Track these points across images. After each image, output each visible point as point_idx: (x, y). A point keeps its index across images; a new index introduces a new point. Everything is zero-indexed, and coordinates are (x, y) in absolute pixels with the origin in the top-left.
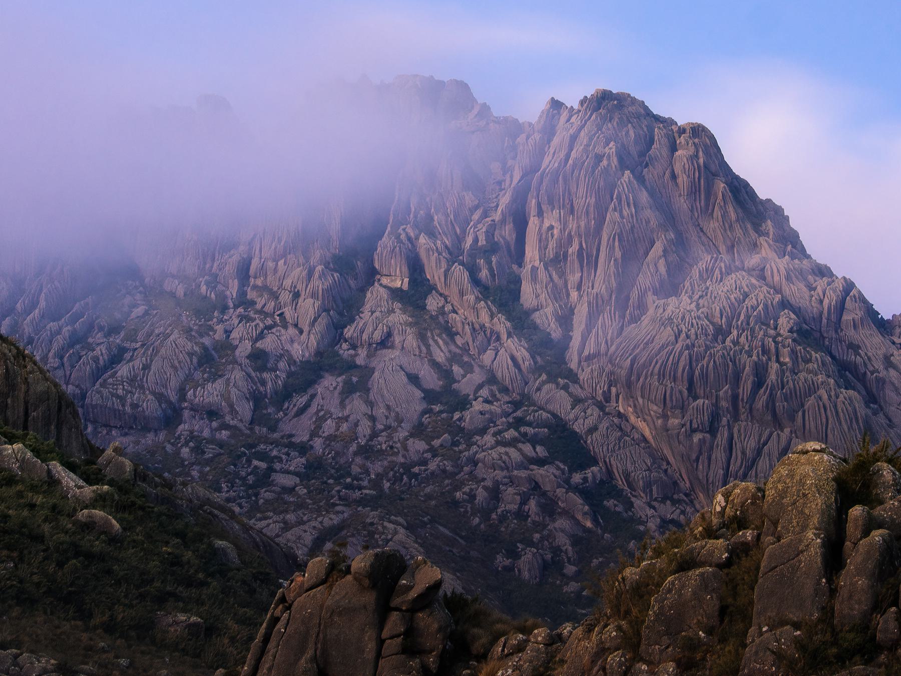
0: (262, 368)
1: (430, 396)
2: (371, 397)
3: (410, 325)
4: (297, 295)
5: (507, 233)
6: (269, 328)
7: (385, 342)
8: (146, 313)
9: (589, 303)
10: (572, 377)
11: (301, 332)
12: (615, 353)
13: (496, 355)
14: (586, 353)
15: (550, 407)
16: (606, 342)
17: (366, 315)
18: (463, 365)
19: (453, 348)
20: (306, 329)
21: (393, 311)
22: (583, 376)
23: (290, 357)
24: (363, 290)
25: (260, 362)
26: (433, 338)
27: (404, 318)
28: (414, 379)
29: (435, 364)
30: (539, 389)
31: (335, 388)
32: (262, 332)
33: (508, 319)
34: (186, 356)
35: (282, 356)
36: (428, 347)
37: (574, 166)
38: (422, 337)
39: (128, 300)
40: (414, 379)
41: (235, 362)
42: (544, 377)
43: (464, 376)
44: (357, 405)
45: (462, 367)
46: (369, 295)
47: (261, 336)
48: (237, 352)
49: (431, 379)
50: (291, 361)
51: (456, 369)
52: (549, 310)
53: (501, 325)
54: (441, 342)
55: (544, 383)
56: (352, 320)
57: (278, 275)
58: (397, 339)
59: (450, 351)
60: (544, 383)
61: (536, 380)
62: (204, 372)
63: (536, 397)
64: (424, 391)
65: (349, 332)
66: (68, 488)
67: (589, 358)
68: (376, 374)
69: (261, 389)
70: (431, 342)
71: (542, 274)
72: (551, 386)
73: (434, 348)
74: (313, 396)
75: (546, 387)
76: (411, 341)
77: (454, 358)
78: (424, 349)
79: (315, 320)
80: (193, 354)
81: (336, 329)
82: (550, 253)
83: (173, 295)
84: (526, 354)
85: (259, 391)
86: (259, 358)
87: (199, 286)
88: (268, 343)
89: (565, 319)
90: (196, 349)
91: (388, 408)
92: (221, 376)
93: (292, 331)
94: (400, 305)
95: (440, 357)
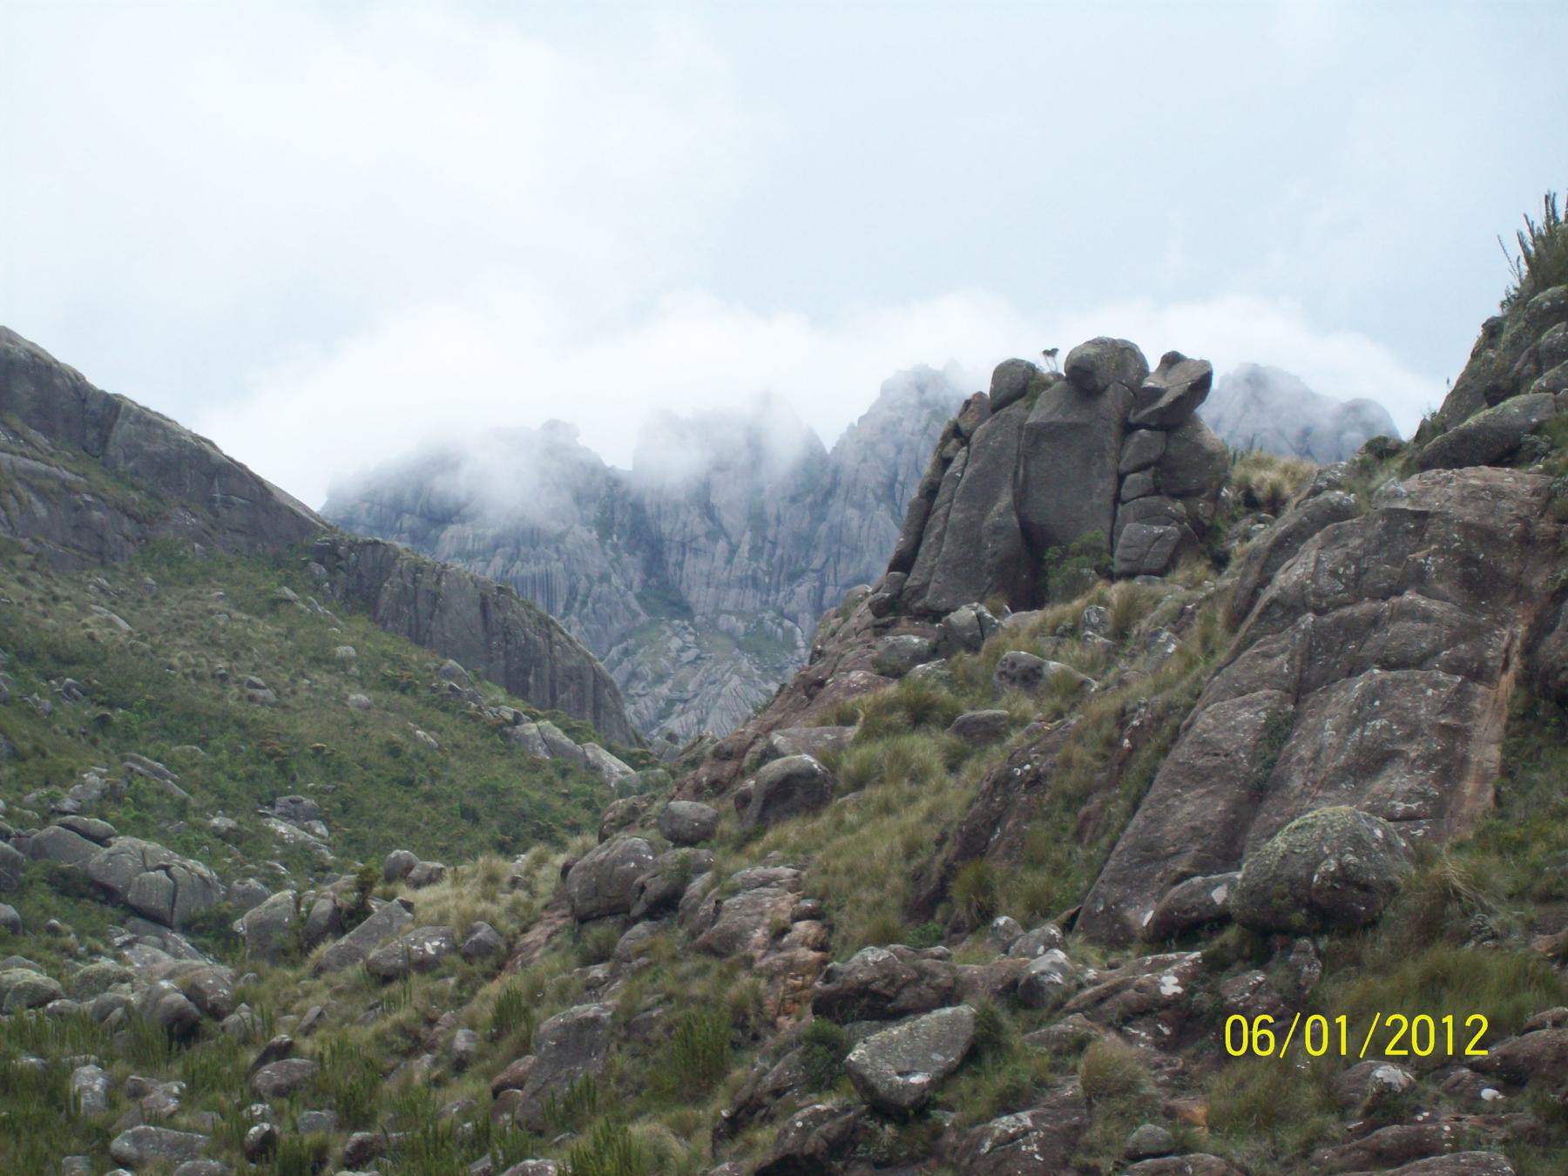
8: (698, 657)
39: (676, 643)
66: (611, 774)
83: (730, 634)
87: (761, 623)
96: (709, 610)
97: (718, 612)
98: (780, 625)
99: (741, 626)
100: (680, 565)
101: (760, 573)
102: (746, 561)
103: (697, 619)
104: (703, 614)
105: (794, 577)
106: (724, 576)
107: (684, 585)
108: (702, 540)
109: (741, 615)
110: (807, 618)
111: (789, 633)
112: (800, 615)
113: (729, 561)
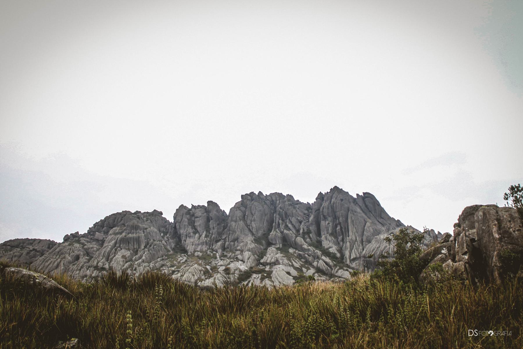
0: (229, 274)
1: (294, 278)
2: (273, 279)
3: (284, 257)
4: (242, 251)
5: (313, 228)
6: (232, 262)
7: (276, 263)
9: (349, 242)
10: (348, 266)
11: (244, 262)
12: (366, 253)
13: (318, 263)
14: (352, 258)
15: (344, 277)
16: (359, 253)
17: (268, 255)
18: (306, 268)
19: (302, 263)
20: (246, 261)
21: (277, 253)
22: (354, 265)
23: (240, 269)
24: (266, 249)
25: (228, 272)
26: (293, 260)
27: (282, 255)
28: (288, 273)
29: (296, 268)
30: (337, 272)
31: (258, 278)
32: (229, 263)
33: (320, 251)
34: (199, 271)
35: (236, 269)
36: (292, 263)
37: (334, 203)
38: (289, 260)
40: (288, 273)
41: (218, 272)
42: (338, 268)
43: (307, 271)
44: (267, 282)
45: (306, 268)
46: (268, 250)
47: (229, 264)
48: (219, 270)
49: (294, 273)
50: (240, 271)
51: (304, 270)
52: (334, 248)
53: (319, 253)
54: (296, 261)
55: (338, 270)
56: (262, 258)
57: (235, 246)
58: (281, 261)
59: (300, 264)
60: (338, 270)
61: (335, 269)
62: (205, 276)
63: (337, 274)
64: (293, 276)
65: (262, 261)
67: (354, 260)
68: (274, 272)
69: (229, 280)
70: (293, 261)
71: (330, 238)
72: (342, 270)
73: (294, 263)
74: (249, 282)
75: (340, 271)
76: (286, 261)
77: (302, 266)
78: (290, 264)
79: (249, 258)
80: (201, 271)
81: (258, 261)
82: (330, 231)
83: (198, 256)
84: (330, 261)
85: (228, 281)
86: (227, 271)
88: (232, 266)
89: (340, 251)
90: (203, 269)
91: (280, 282)
92: (212, 277)
93: (240, 262)
94: (279, 252)
95: (297, 265)
96: (192, 251)
97: (195, 251)
98: (212, 253)
99: (201, 254)
100: (185, 241)
101: (208, 241)
102: (203, 238)
103: (189, 253)
104: (191, 252)
105: (217, 241)
106: (197, 242)
107: (186, 245)
108: (192, 234)
109: (201, 252)
110: (220, 251)
111: (215, 255)
112: (218, 250)
113: (199, 239)
